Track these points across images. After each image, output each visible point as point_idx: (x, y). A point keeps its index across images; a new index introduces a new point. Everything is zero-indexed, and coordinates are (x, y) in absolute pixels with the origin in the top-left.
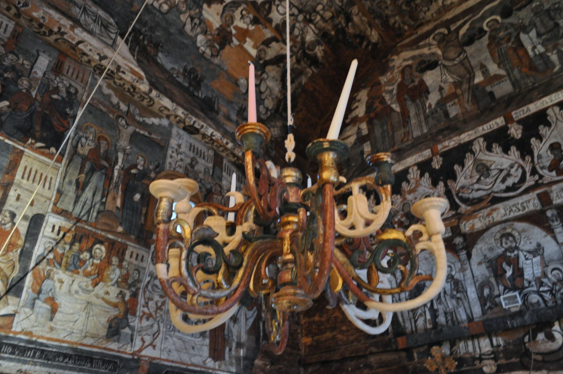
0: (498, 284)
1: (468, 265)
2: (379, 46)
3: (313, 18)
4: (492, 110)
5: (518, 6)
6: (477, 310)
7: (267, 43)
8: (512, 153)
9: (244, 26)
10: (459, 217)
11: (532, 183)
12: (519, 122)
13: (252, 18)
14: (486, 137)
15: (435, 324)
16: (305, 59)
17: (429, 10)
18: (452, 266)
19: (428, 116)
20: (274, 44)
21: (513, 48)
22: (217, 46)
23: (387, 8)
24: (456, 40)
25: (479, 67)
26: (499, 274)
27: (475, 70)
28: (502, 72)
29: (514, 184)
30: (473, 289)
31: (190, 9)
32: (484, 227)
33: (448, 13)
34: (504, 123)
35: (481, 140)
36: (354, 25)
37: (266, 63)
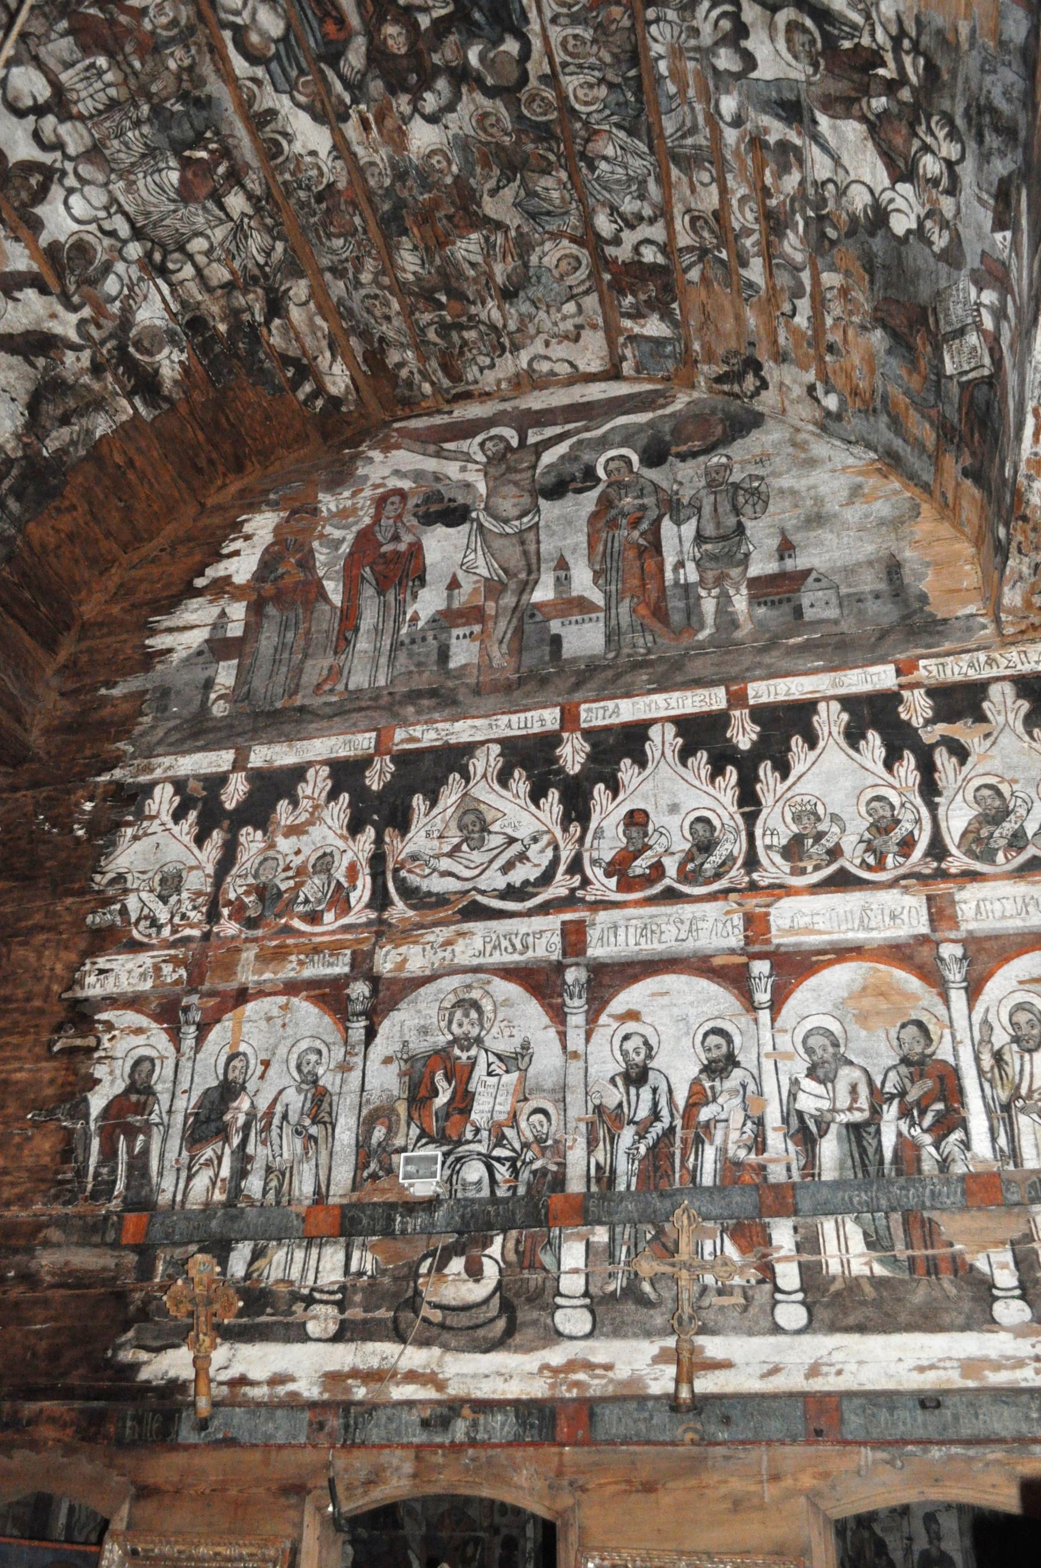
0: (410, 1118)
1: (359, 1060)
2: (344, 409)
3: (171, 266)
4: (544, 681)
5: (683, 448)
6: (343, 1175)
8: (547, 807)
10: (382, 930)
11: (564, 892)
12: (588, 734)
14: (508, 744)
15: (235, 1192)
16: (121, 370)
17: (492, 366)
18: (325, 1051)
19: (402, 644)
20: (30, 294)
21: (639, 546)
23: (388, 318)
24: (529, 473)
25: (553, 564)
26: (419, 1094)
27: (543, 566)
28: (597, 597)
29: (526, 883)
30: (353, 1122)
32: (428, 973)
33: (536, 393)
34: (557, 726)
35: (496, 749)
36: (289, 326)
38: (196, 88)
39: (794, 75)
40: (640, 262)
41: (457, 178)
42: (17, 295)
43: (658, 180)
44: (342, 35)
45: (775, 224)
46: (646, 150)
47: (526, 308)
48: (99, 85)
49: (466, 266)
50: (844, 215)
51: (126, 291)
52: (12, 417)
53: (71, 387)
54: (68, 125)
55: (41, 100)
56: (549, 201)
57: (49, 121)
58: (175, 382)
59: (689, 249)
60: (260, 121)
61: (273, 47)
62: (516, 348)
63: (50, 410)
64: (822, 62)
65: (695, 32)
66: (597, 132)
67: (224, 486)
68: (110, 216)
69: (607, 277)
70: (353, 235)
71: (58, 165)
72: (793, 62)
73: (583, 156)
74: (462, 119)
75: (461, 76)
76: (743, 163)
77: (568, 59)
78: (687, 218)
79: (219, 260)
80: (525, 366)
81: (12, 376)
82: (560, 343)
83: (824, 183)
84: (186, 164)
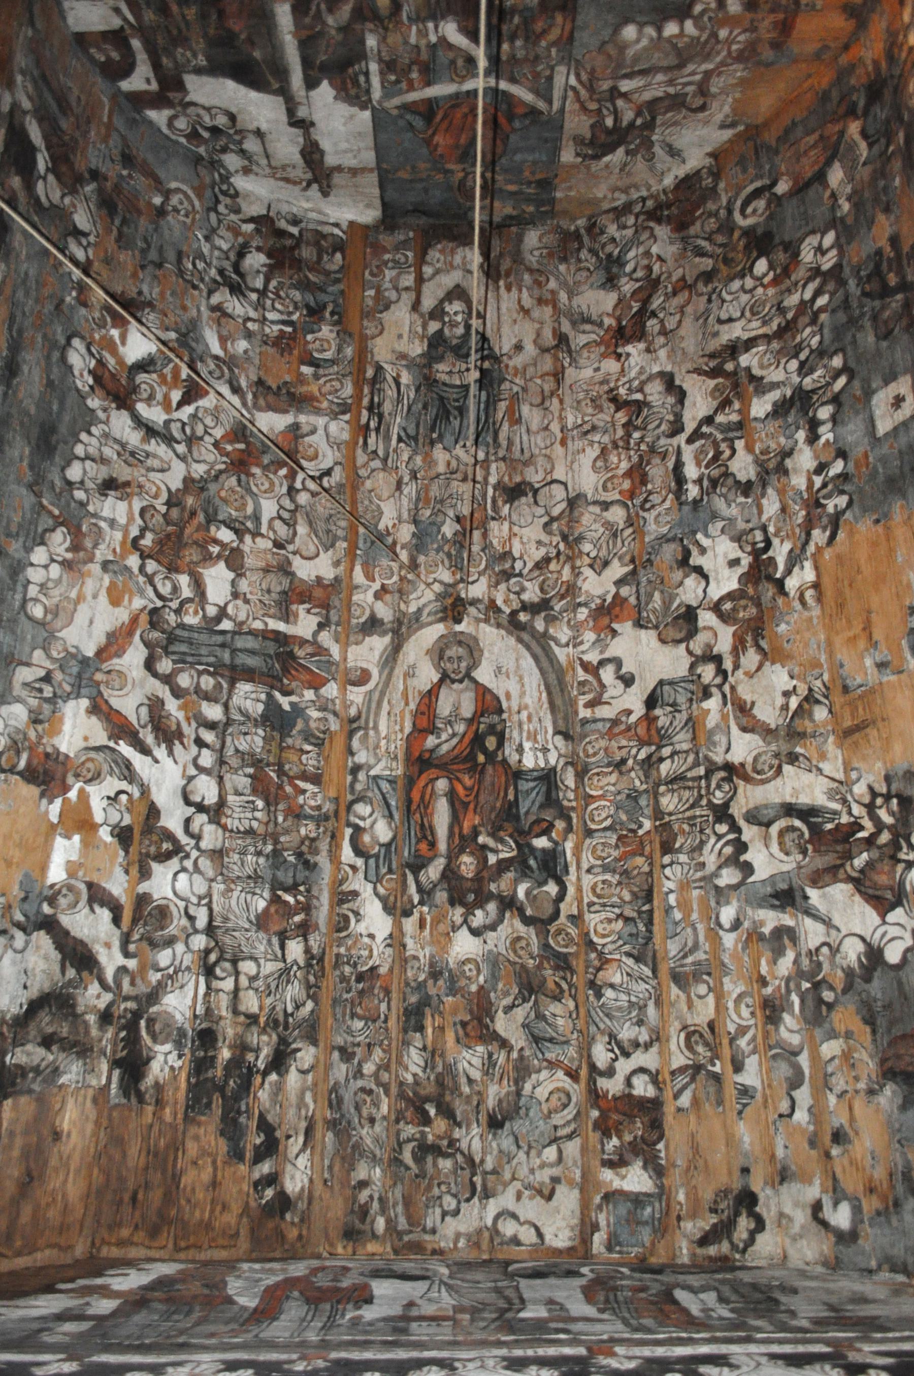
3: (218, 971)
7: (97, 896)
9: (99, 817)
13: (123, 824)
16: (123, 1034)
17: (457, 1212)
20: (105, 915)
22: (22, 764)
31: (61, 668)
36: (279, 1088)
37: (50, 925)
39: (786, 868)
40: (630, 1095)
41: (481, 988)
42: (97, 908)
43: (658, 1003)
44: (430, 854)
45: (772, 1011)
46: (650, 974)
47: (507, 1143)
48: (249, 815)
49: (463, 1080)
50: (840, 973)
51: (171, 971)
52: (13, 999)
53: (76, 1016)
54: (213, 827)
55: (206, 802)
57: (203, 818)
58: (157, 1083)
59: (682, 1070)
62: (487, 1194)
63: (45, 1022)
64: (810, 847)
65: (703, 865)
66: (608, 961)
68: (199, 905)
71: (188, 848)
72: (785, 858)
73: (592, 984)
74: (499, 939)
77: (595, 900)
78: (683, 1035)
80: (489, 1223)
81: (42, 965)
82: (531, 1198)
83: (817, 949)
84: (275, 900)
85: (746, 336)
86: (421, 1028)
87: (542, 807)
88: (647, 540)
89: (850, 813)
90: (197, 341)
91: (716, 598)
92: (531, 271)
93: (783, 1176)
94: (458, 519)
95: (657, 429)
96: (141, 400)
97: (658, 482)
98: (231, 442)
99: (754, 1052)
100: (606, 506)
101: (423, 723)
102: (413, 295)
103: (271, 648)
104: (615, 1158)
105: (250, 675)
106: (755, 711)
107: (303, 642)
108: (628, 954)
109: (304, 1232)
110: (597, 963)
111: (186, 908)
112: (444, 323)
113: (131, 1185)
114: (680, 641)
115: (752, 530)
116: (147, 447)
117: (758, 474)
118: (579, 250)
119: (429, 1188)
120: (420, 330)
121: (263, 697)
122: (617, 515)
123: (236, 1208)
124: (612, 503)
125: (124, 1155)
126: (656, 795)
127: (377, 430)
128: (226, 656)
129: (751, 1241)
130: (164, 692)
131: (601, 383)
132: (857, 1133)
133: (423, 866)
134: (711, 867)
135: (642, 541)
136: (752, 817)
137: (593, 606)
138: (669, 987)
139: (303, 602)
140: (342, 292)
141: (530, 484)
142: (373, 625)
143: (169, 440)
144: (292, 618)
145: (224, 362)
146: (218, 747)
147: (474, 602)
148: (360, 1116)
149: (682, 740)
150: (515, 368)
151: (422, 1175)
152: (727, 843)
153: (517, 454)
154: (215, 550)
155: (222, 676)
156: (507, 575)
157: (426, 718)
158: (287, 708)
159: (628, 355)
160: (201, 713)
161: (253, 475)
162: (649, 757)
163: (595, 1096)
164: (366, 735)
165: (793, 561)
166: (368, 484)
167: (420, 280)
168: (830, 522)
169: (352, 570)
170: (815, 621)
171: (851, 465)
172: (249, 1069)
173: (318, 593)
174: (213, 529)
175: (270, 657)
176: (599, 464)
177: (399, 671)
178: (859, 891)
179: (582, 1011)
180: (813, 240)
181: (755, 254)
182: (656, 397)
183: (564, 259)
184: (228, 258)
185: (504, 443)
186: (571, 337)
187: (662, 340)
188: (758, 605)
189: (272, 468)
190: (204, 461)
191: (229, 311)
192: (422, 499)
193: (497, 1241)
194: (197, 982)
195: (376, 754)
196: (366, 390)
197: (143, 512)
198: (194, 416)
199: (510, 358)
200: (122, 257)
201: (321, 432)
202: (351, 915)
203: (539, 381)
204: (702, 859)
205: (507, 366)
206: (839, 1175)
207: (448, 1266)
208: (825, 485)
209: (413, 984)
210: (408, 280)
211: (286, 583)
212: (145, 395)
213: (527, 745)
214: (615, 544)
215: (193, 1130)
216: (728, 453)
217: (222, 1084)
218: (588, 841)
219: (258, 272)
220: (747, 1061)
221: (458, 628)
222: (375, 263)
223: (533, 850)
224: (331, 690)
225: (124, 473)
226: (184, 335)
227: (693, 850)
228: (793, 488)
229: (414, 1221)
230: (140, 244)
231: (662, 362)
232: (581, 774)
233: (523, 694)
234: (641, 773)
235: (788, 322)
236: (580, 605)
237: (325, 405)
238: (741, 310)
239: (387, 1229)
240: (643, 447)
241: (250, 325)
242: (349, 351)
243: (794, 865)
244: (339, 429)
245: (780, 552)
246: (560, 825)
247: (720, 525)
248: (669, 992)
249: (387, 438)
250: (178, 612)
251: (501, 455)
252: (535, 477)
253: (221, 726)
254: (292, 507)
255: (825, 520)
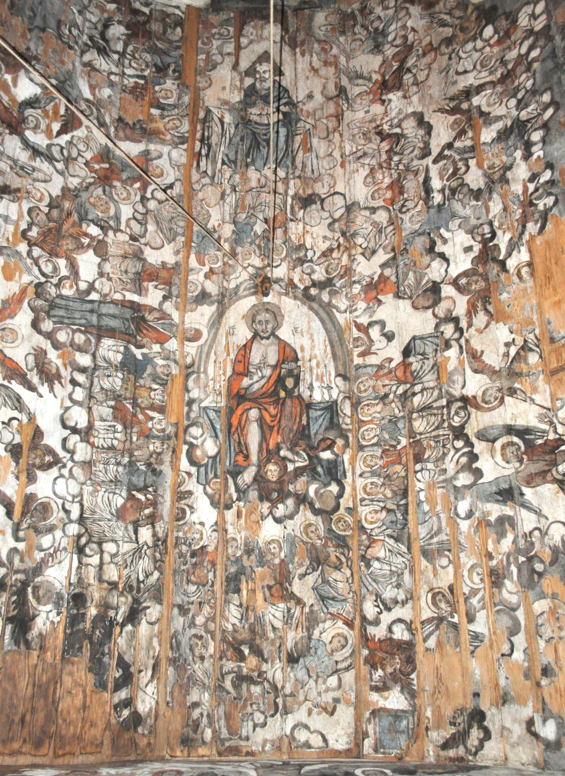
3: (87, 551)
13: (15, 442)
16: (14, 598)
17: (264, 725)
36: (133, 636)
38: (157, 463)
39: (507, 472)
40: (391, 639)
41: (282, 561)
43: (412, 572)
44: (245, 464)
45: (496, 578)
46: (406, 550)
47: (301, 674)
48: (111, 436)
49: (269, 628)
50: (547, 550)
51: (51, 551)
54: (84, 444)
55: (79, 426)
56: (335, 588)
58: (41, 634)
59: (429, 620)
60: (182, 495)
61: (206, 459)
62: (286, 712)
64: (525, 457)
65: (445, 471)
66: (375, 541)
67: (18, 752)
68: (73, 502)
69: (365, 652)
70: (204, 585)
71: (65, 460)
72: (506, 465)
73: (363, 558)
74: (295, 526)
75: (302, 499)
76: (472, 541)
77: (366, 496)
78: (430, 595)
79: (116, 564)
80: (288, 732)
82: (319, 713)
83: (531, 533)
84: (131, 497)
85: (476, 83)
86: (238, 591)
87: (327, 429)
88: (404, 234)
89: (556, 432)
90: (72, 87)
91: (454, 276)
92: (319, 41)
93: (504, 699)
94: (266, 221)
95: (410, 155)
96: (28, 129)
97: (412, 193)
98: (98, 163)
99: (483, 608)
100: (373, 210)
101: (240, 368)
102: (233, 58)
103: (128, 313)
104: (380, 684)
105: (112, 333)
106: (484, 358)
107: (152, 310)
108: (390, 536)
109: (152, 741)
110: (367, 543)
111: (63, 504)
112: (256, 79)
113: (21, 709)
114: (428, 308)
115: (482, 225)
116: (33, 164)
117: (486, 184)
118: (354, 26)
119: (244, 706)
120: (238, 83)
121: (122, 349)
122: (382, 217)
123: (101, 725)
124: (378, 208)
125: (15, 686)
126: (410, 420)
127: (207, 156)
128: (94, 319)
129: (481, 746)
130: (46, 345)
131: (371, 122)
132: (561, 669)
133: (239, 473)
134: (451, 472)
135: (400, 235)
136: (482, 436)
137: (364, 283)
138: (420, 560)
139: (152, 281)
140: (181, 56)
141: (318, 195)
142: (203, 297)
143: (51, 159)
144: (143, 292)
145: (93, 104)
146: (88, 385)
147: (277, 281)
148: (194, 655)
149: (430, 380)
150: (308, 112)
151: (238, 698)
152: (463, 455)
153: (309, 173)
154: (86, 241)
155: (91, 333)
156: (302, 261)
157: (242, 365)
158: (140, 357)
159: (390, 101)
160: (75, 361)
161: (115, 187)
162: (406, 392)
163: (365, 639)
164: (199, 377)
165: (513, 246)
166: (200, 195)
167: (238, 48)
168: (541, 217)
169: (188, 257)
170: (529, 290)
171: (557, 174)
172: (111, 622)
173: (163, 274)
174: (84, 226)
175: (127, 320)
176: (369, 180)
177: (222, 331)
178: (562, 489)
179: (356, 577)
180: (528, 9)
181: (484, 22)
182: (411, 130)
183: (343, 33)
184: (96, 28)
185: (300, 166)
186: (348, 89)
187: (415, 89)
188: (486, 280)
189: (129, 183)
190: (78, 176)
191: (97, 67)
192: (239, 206)
193: (294, 745)
194: (72, 559)
195: (205, 391)
196: (199, 127)
197: (30, 211)
198: (70, 143)
199: (304, 104)
200: (14, 21)
201: (165, 156)
202: (187, 509)
203: (325, 121)
204: (444, 467)
205: (302, 110)
206: (547, 700)
207: (256, 770)
208: (536, 190)
209: (232, 559)
210: (230, 48)
211: (139, 266)
212: (32, 125)
213: (316, 384)
214: (380, 238)
215: (68, 668)
216: (463, 169)
217: (91, 633)
218: (360, 454)
219: (119, 39)
220: (478, 614)
221: (266, 299)
222: (206, 35)
223: (320, 460)
224: (172, 345)
225: (15, 182)
226: (63, 82)
227: (437, 460)
228: (513, 193)
229: (233, 732)
230: (28, 13)
231: (415, 105)
232: (355, 406)
233: (313, 348)
234: (399, 404)
235: (509, 71)
236: (354, 282)
237: (168, 137)
238: (473, 64)
239: (213, 738)
240: (401, 167)
241: (112, 77)
242: (186, 99)
243: (513, 470)
244: (179, 155)
245: (503, 240)
246: (340, 442)
247: (457, 222)
248: (420, 564)
249: (214, 162)
250: (57, 286)
251: (297, 174)
252: (322, 190)
253: (90, 370)
254: (144, 211)
255: (537, 216)
